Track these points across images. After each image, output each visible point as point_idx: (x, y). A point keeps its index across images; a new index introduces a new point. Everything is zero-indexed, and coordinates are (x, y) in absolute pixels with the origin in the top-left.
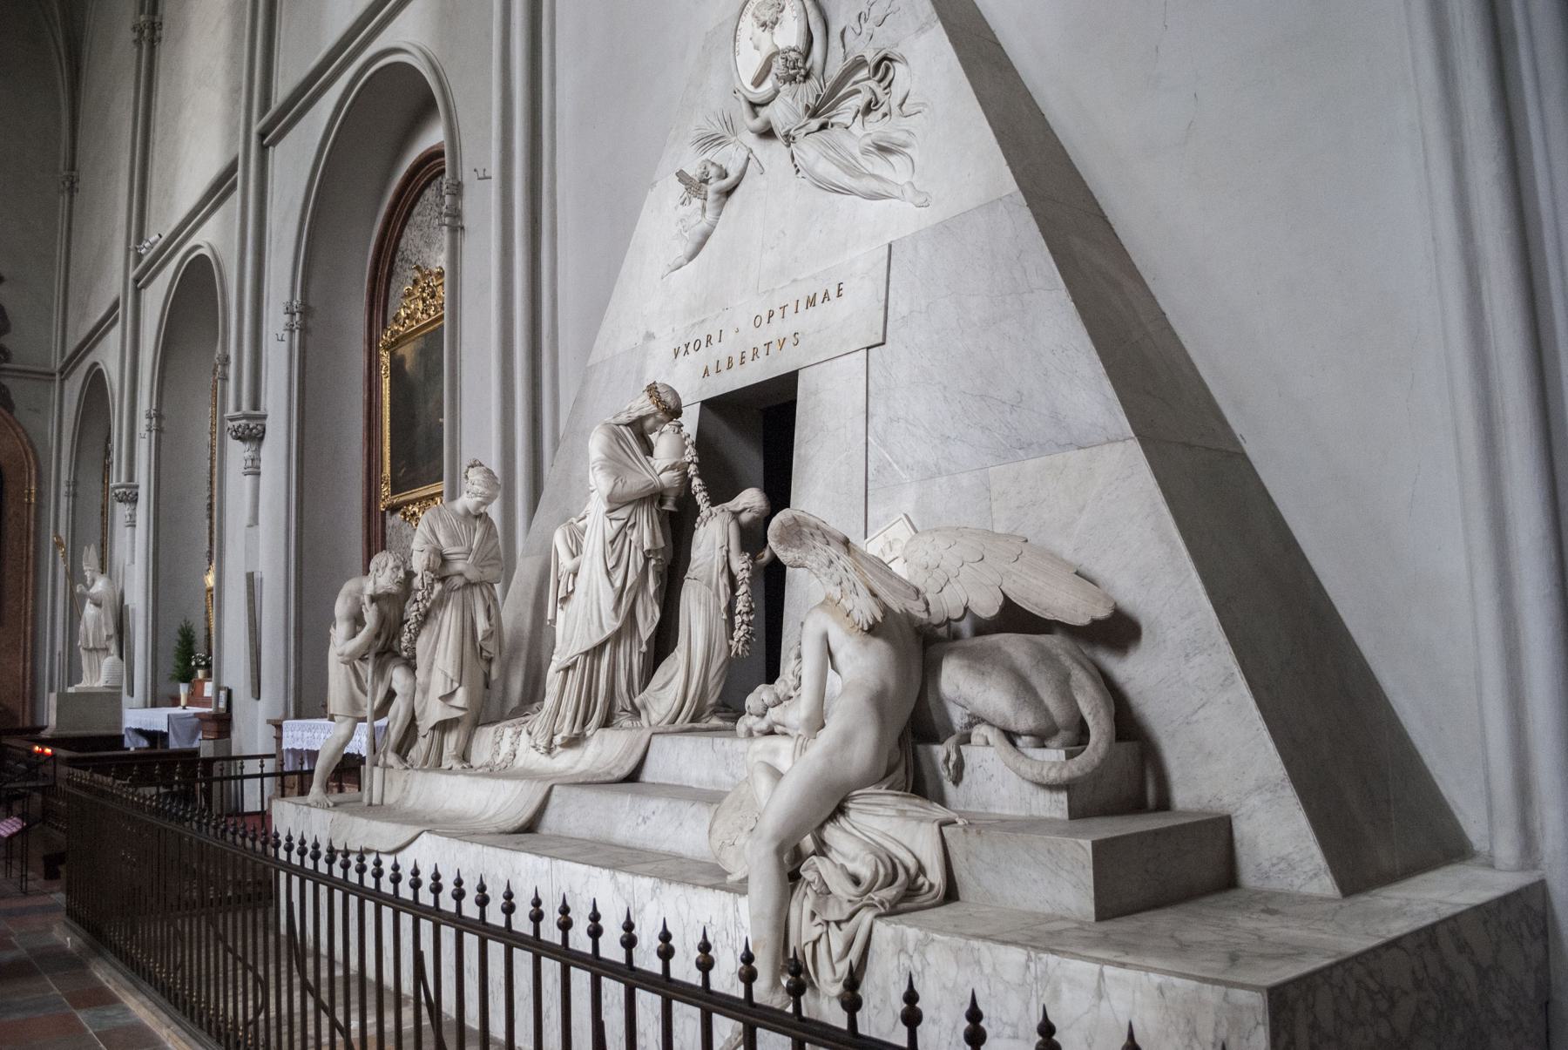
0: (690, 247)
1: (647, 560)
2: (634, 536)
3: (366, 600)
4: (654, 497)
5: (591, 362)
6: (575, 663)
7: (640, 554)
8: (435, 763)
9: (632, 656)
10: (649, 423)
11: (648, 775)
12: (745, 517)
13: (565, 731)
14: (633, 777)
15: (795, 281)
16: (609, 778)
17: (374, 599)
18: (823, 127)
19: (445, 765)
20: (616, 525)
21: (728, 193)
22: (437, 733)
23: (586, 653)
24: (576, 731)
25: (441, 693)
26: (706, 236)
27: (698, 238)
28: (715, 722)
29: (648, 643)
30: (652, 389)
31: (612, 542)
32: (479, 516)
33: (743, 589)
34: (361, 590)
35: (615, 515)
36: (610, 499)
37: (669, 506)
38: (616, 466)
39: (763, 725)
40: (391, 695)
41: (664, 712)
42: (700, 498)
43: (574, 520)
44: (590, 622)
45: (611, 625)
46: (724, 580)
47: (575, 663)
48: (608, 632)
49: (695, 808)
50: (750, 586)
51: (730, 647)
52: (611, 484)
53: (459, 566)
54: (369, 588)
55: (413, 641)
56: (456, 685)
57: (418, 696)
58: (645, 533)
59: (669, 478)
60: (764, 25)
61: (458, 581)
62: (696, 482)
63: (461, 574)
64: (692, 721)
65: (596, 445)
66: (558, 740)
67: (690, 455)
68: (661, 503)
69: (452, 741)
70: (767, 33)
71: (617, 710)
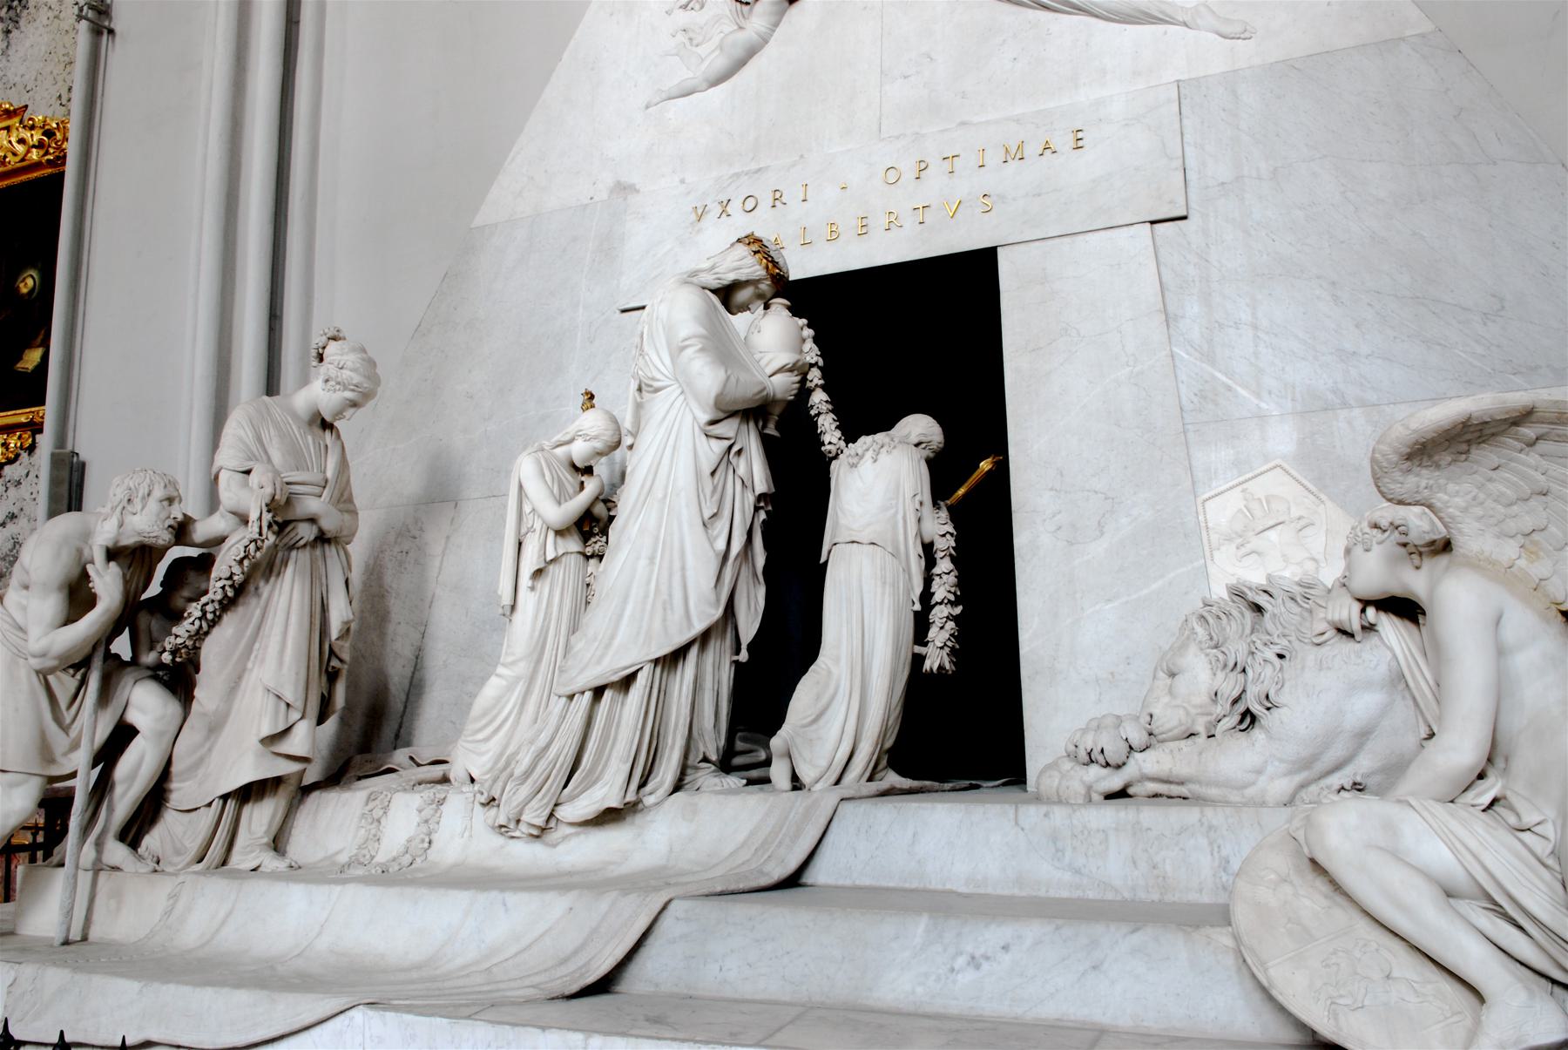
0: (720, 63)
1: (757, 509)
2: (742, 470)
3: (99, 556)
4: (755, 412)
5: (478, 221)
8: (217, 855)
9: (715, 673)
10: (743, 295)
11: (819, 874)
12: (927, 453)
13: (607, 791)
14: (793, 881)
15: (963, 123)
16: (764, 882)
17: (112, 554)
19: (239, 860)
20: (718, 447)
22: (231, 804)
23: (656, 661)
24: (631, 797)
25: (266, 730)
26: (751, 52)
27: (739, 52)
28: (892, 779)
29: (750, 647)
30: (756, 245)
31: (713, 473)
32: (326, 426)
33: (944, 565)
34: (86, 535)
35: (718, 429)
36: (718, 403)
37: (771, 430)
38: (722, 349)
39: (1115, 782)
40: (124, 734)
41: (824, 763)
42: (828, 428)
43: (547, 444)
44: (667, 606)
45: (705, 614)
46: (915, 550)
47: (627, 682)
48: (699, 627)
49: (1137, 938)
50: (953, 560)
51: (918, 660)
52: (721, 374)
53: (312, 505)
55: (200, 636)
56: (295, 715)
58: (755, 470)
59: (782, 386)
61: (306, 532)
62: (819, 398)
63: (312, 520)
64: (870, 779)
65: (680, 311)
66: (567, 812)
67: (812, 353)
68: (764, 426)
69: (260, 817)
71: (692, 760)
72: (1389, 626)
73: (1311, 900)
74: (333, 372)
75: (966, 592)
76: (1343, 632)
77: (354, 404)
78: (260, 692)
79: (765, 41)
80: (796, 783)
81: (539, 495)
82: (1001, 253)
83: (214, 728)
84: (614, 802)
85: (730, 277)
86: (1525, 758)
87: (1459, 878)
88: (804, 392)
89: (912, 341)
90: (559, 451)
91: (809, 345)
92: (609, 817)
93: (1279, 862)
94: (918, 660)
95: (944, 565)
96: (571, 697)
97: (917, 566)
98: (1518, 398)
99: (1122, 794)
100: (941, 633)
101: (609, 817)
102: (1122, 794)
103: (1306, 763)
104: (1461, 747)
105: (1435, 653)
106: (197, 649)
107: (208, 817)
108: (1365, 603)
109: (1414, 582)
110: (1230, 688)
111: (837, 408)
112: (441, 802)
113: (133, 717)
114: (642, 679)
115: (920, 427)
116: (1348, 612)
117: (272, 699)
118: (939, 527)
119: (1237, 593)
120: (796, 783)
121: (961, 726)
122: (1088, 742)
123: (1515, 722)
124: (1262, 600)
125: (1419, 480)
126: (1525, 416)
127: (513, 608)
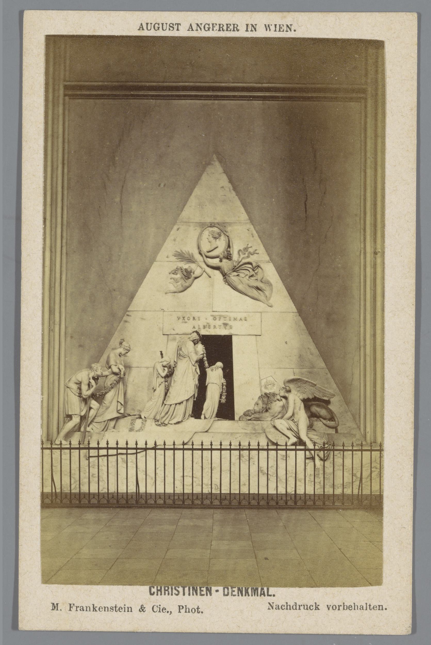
0: (181, 289)
3: (91, 378)
6: (182, 402)
7: (197, 376)
14: (206, 432)
18: (238, 275)
21: (196, 278)
28: (217, 419)
38: (196, 353)
39: (249, 418)
54: (91, 376)
55: (106, 393)
57: (101, 410)
60: (215, 238)
62: (205, 358)
69: (112, 424)
70: (214, 240)
72: (284, 400)
73: (273, 430)
74: (126, 348)
75: (227, 392)
76: (278, 400)
77: (127, 353)
78: (116, 403)
79: (190, 286)
80: (205, 418)
81: (160, 371)
82: (233, 337)
83: (107, 408)
84: (180, 420)
85: (195, 339)
86: (296, 416)
87: (288, 427)
88: (203, 357)
89: (218, 349)
90: (162, 363)
91: (204, 350)
92: (178, 423)
93: (271, 426)
94: (220, 401)
95: (224, 387)
96: (171, 405)
97: (221, 387)
98: (299, 377)
99: (250, 420)
100: (224, 397)
101: (178, 423)
102: (250, 420)
103: (273, 416)
104: (289, 414)
105: (288, 403)
106: (105, 395)
107: (106, 423)
108: (281, 397)
109: (287, 395)
110: (264, 406)
111: (208, 360)
112: (146, 421)
113: (92, 406)
114: (185, 403)
115: (219, 364)
116: (278, 397)
117: (119, 404)
118: (223, 381)
119: (265, 394)
120: (205, 418)
121: (226, 411)
122: (247, 413)
123: (296, 411)
124: (268, 395)
125: (287, 385)
126: (299, 379)
127: (155, 390)
